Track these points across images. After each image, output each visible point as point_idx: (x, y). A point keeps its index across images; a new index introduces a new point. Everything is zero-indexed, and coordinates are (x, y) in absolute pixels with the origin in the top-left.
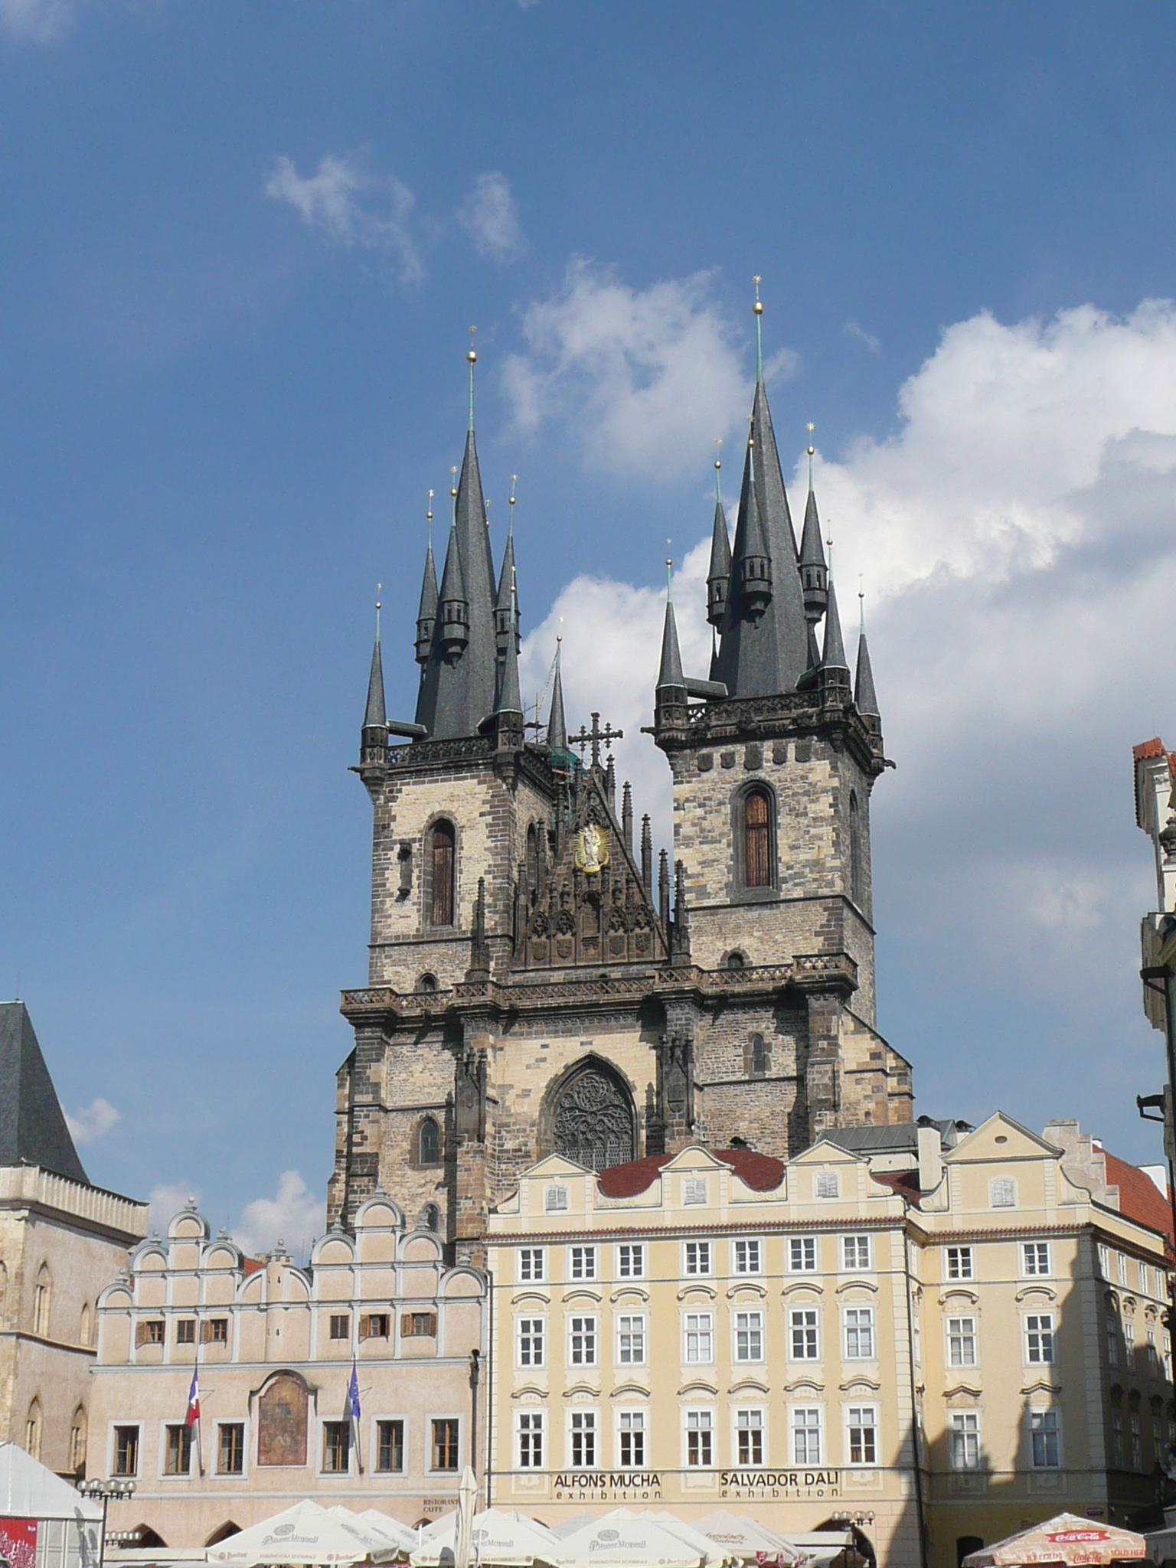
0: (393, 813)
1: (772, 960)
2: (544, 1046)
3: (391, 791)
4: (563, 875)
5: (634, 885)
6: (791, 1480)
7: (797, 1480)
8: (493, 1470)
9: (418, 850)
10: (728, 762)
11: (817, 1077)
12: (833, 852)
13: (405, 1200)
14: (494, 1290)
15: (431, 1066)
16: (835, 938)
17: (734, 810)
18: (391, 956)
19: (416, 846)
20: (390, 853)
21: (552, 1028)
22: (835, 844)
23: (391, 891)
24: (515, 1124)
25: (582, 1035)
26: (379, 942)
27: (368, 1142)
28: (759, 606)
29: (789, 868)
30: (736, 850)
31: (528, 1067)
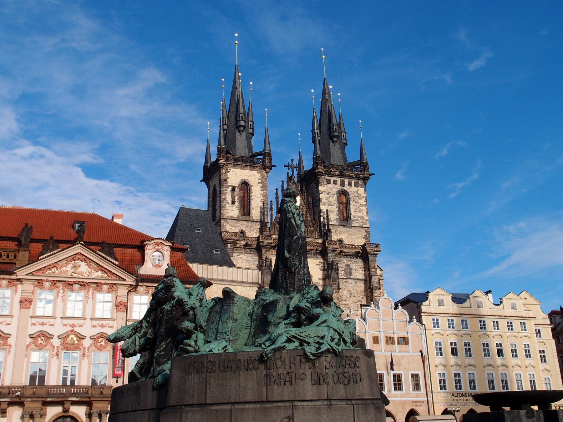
0: (228, 176)
1: (350, 244)
3: (227, 169)
5: (308, 214)
8: (433, 391)
10: (335, 182)
11: (375, 280)
14: (426, 331)
15: (244, 261)
16: (367, 240)
17: (337, 196)
18: (229, 223)
19: (236, 188)
20: (227, 189)
22: (367, 213)
26: (224, 218)
28: (335, 139)
29: (354, 217)
30: (338, 209)
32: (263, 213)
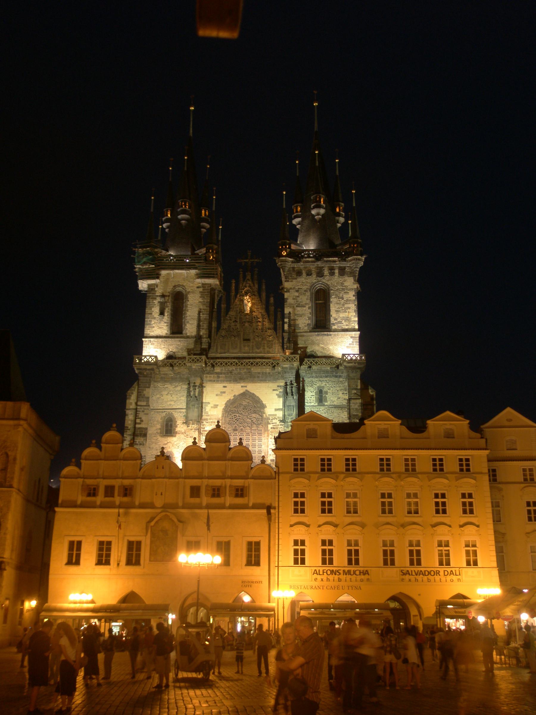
2: (225, 387)
4: (233, 315)
5: (266, 320)
6: (437, 573)
7: (440, 573)
8: (279, 566)
9: (168, 300)
10: (309, 274)
12: (355, 315)
13: (157, 450)
14: (280, 476)
15: (171, 392)
17: (311, 294)
21: (228, 379)
23: (155, 316)
24: (210, 419)
25: (242, 383)
27: (142, 423)
29: (335, 319)
31: (217, 395)
32: (199, 326)
